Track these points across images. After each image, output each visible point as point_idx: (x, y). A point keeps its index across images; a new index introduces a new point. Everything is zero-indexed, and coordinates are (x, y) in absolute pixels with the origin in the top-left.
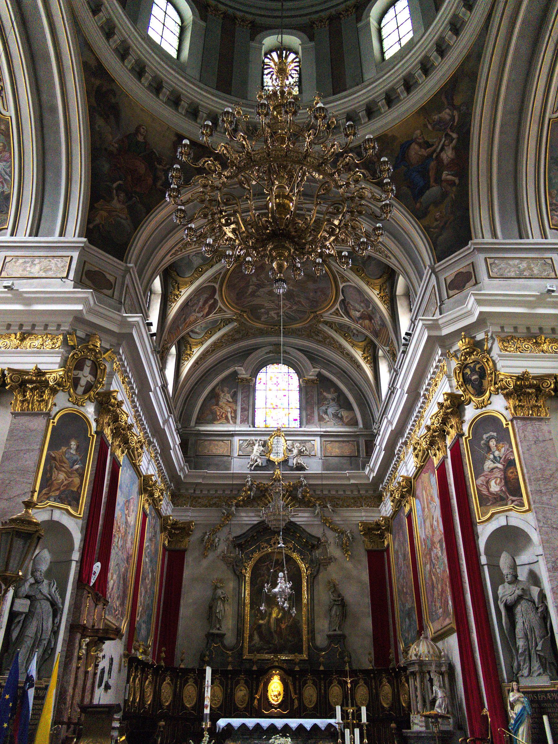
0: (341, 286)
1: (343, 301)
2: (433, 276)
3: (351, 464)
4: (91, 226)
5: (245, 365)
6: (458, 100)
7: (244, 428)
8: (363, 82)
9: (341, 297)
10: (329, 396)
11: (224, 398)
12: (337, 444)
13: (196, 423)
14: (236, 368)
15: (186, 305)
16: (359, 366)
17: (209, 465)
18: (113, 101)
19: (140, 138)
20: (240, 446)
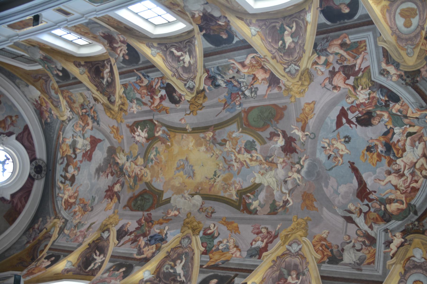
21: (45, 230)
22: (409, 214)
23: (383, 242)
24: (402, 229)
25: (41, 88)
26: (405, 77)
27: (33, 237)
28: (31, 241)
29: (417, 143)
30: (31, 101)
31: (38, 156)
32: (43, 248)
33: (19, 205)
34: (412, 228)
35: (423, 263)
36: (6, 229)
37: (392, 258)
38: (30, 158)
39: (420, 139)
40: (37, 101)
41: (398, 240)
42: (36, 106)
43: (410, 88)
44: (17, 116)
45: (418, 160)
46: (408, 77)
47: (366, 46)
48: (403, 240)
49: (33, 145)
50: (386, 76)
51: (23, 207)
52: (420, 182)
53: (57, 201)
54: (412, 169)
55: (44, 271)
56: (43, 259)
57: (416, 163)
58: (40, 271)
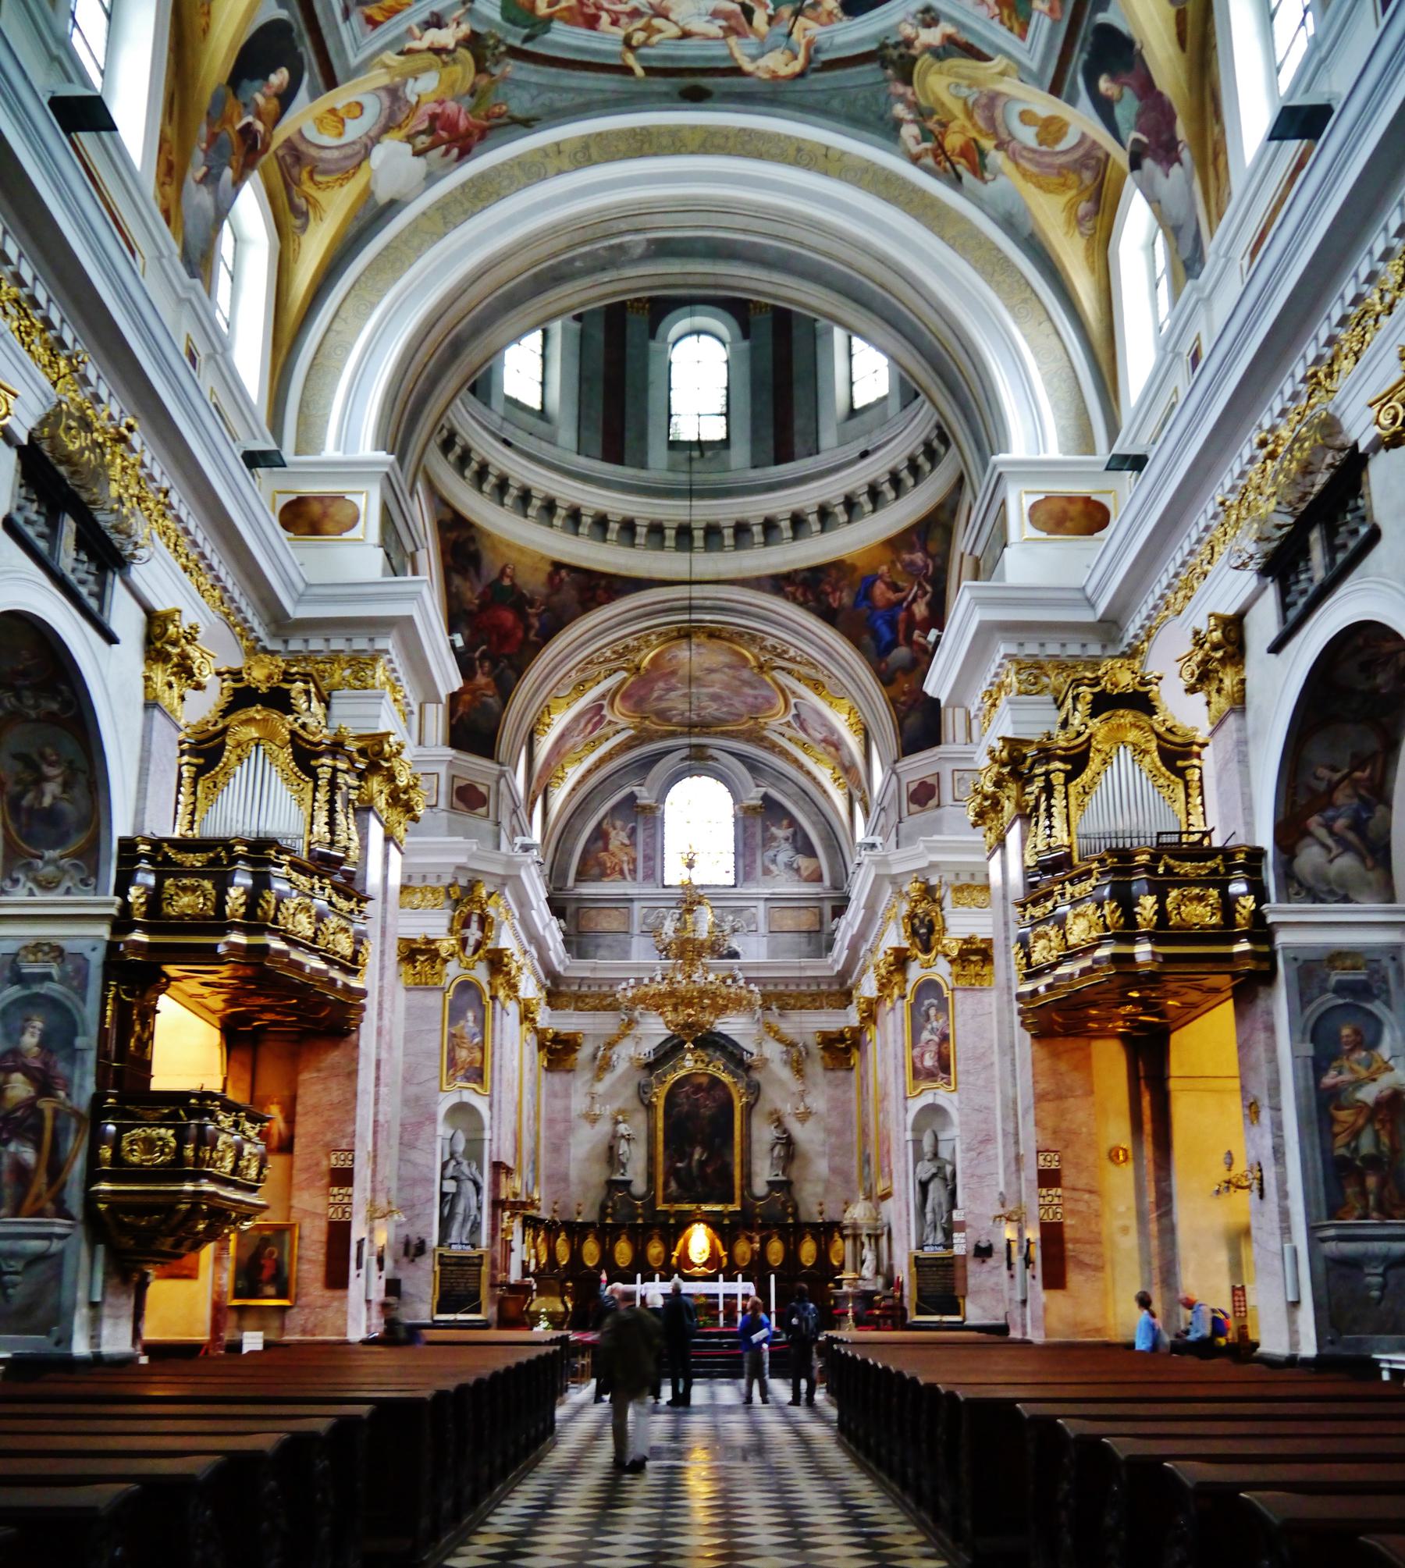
0: (793, 701)
1: (797, 716)
2: (894, 778)
3: (809, 943)
4: (454, 721)
5: (648, 781)
6: (933, 547)
7: (649, 890)
8: (818, 452)
9: (793, 711)
10: (781, 832)
11: (618, 837)
12: (789, 913)
13: (577, 880)
14: (635, 789)
15: (562, 736)
16: (825, 791)
17: (598, 946)
18: (472, 548)
19: (507, 582)
20: (645, 917)
22: (525, 27)
23: (436, 8)
24: (481, 29)
26: (903, 50)
29: (723, 23)
34: (488, 47)
35: (407, 101)
37: (401, 53)
39: (730, 31)
41: (446, 37)
43: (873, 47)
45: (676, 23)
46: (901, 56)
47: (1011, 29)
48: (451, 46)
50: (920, 16)
52: (614, 29)
54: (651, 12)
57: (667, 18)
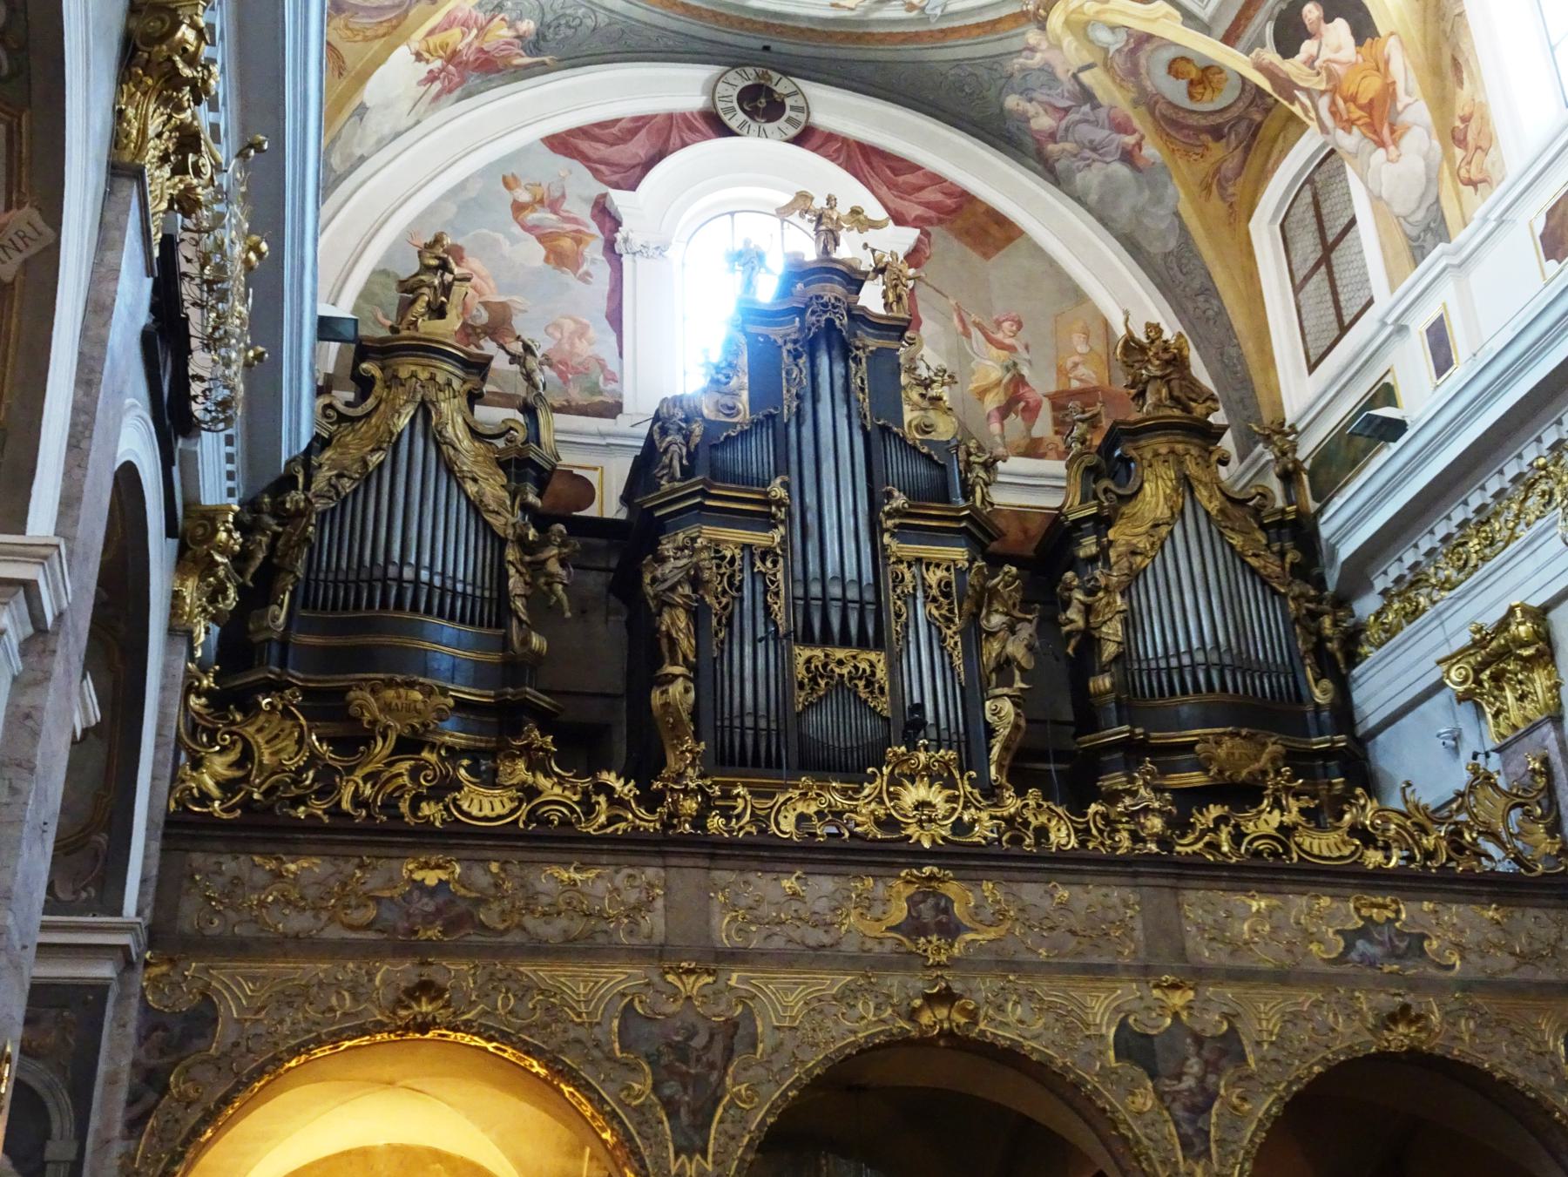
21: (1085, 77)
25: (377, 37)
27: (1100, 135)
28: (1130, 140)
30: (421, 107)
31: (694, 101)
32: (1183, 83)
33: (932, 195)
36: (1038, 251)
38: (709, 138)
40: (432, 78)
42: (450, 91)
44: (508, 183)
49: (640, 123)
51: (936, 179)
53: (945, 16)
55: (1392, 49)
56: (1292, 67)
58: (1381, 67)
